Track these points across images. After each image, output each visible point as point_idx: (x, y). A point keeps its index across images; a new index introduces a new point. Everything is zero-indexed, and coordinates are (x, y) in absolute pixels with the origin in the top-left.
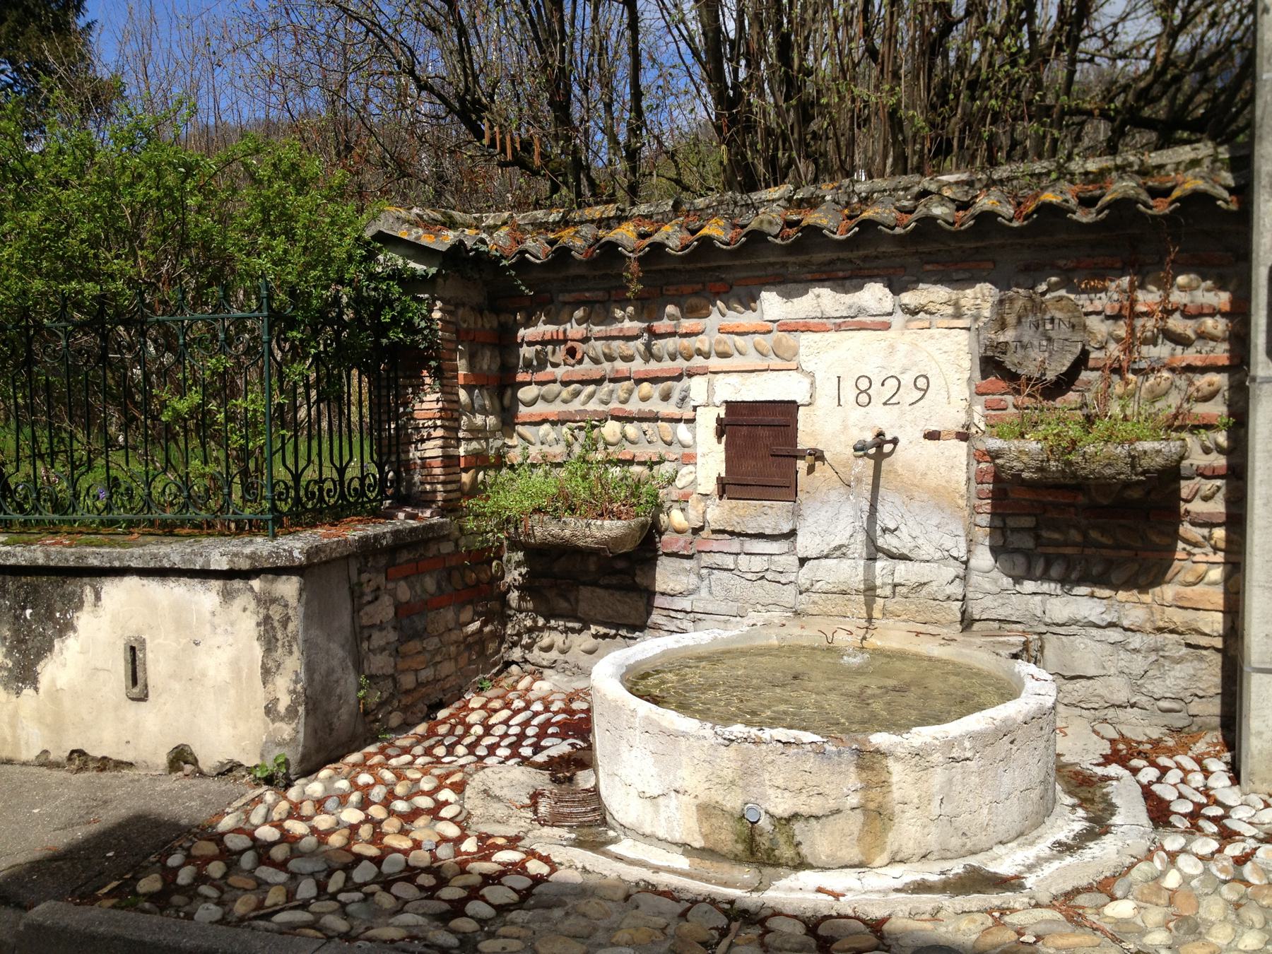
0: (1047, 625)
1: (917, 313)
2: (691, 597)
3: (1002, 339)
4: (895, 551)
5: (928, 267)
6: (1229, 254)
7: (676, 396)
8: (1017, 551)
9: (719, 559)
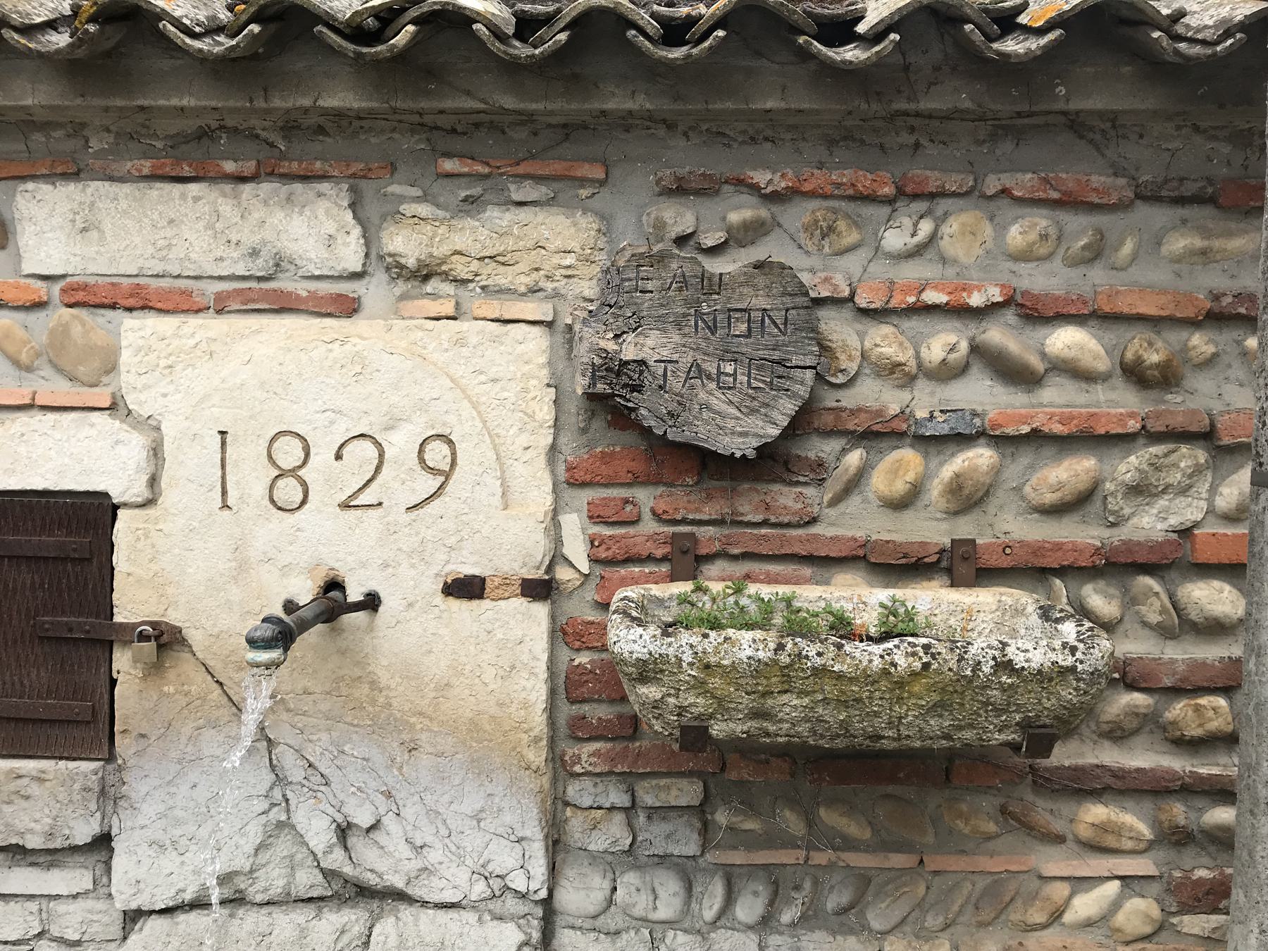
1: (426, 278)
3: (629, 353)
4: (372, 880)
5: (449, 165)
6: (1122, 181)
8: (663, 860)
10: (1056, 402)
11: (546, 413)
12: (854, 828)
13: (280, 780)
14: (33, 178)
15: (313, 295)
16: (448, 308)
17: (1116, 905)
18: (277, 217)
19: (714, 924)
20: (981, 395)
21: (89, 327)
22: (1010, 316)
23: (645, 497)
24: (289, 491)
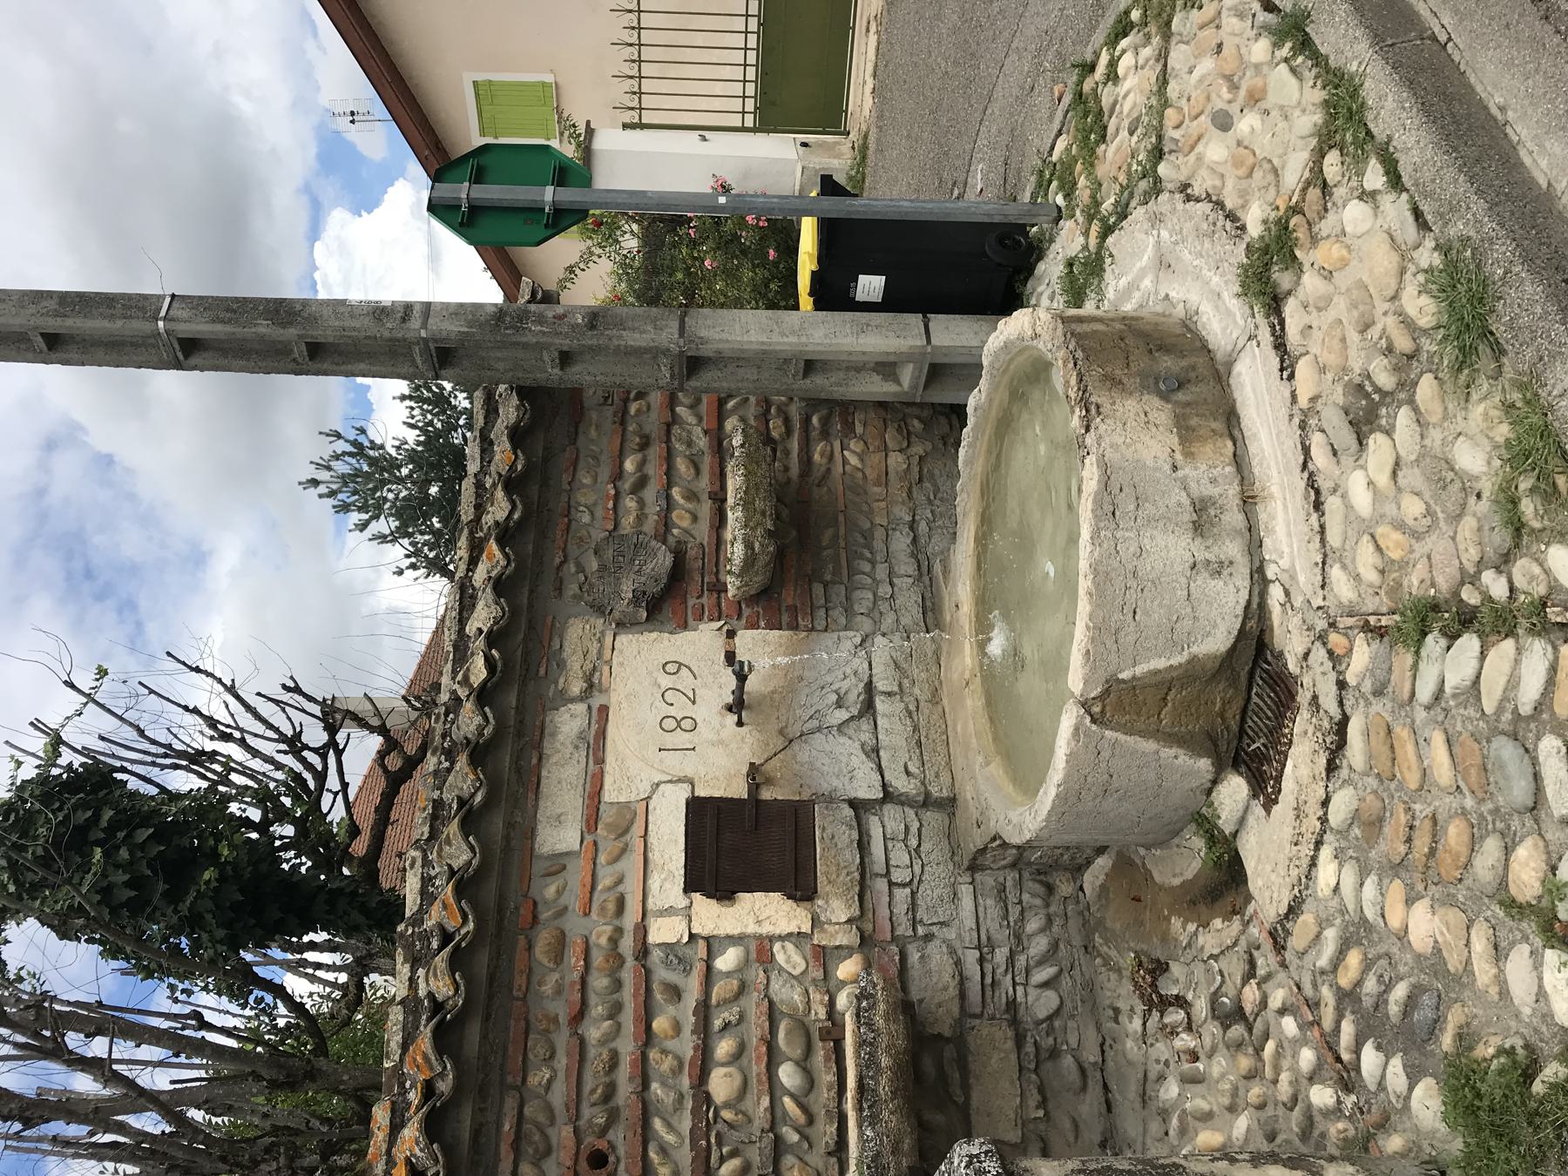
0: (921, 575)
2: (960, 952)
5: (542, 672)
7: (673, 977)
9: (901, 908)
10: (654, 470)
11: (655, 635)
12: (829, 533)
13: (819, 729)
14: (532, 849)
15: (598, 722)
16: (606, 669)
17: (854, 452)
18: (561, 737)
19: (874, 580)
20: (650, 493)
21: (607, 815)
22: (619, 484)
23: (691, 602)
24: (687, 724)
